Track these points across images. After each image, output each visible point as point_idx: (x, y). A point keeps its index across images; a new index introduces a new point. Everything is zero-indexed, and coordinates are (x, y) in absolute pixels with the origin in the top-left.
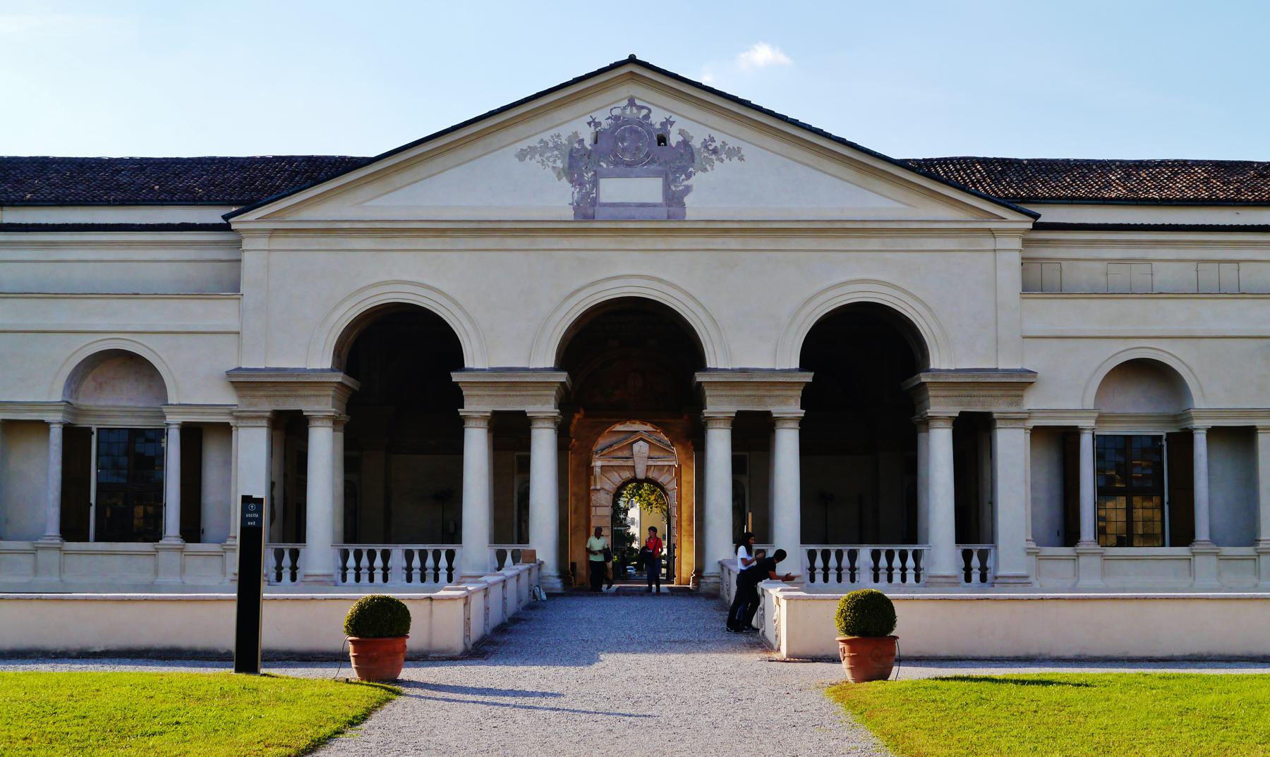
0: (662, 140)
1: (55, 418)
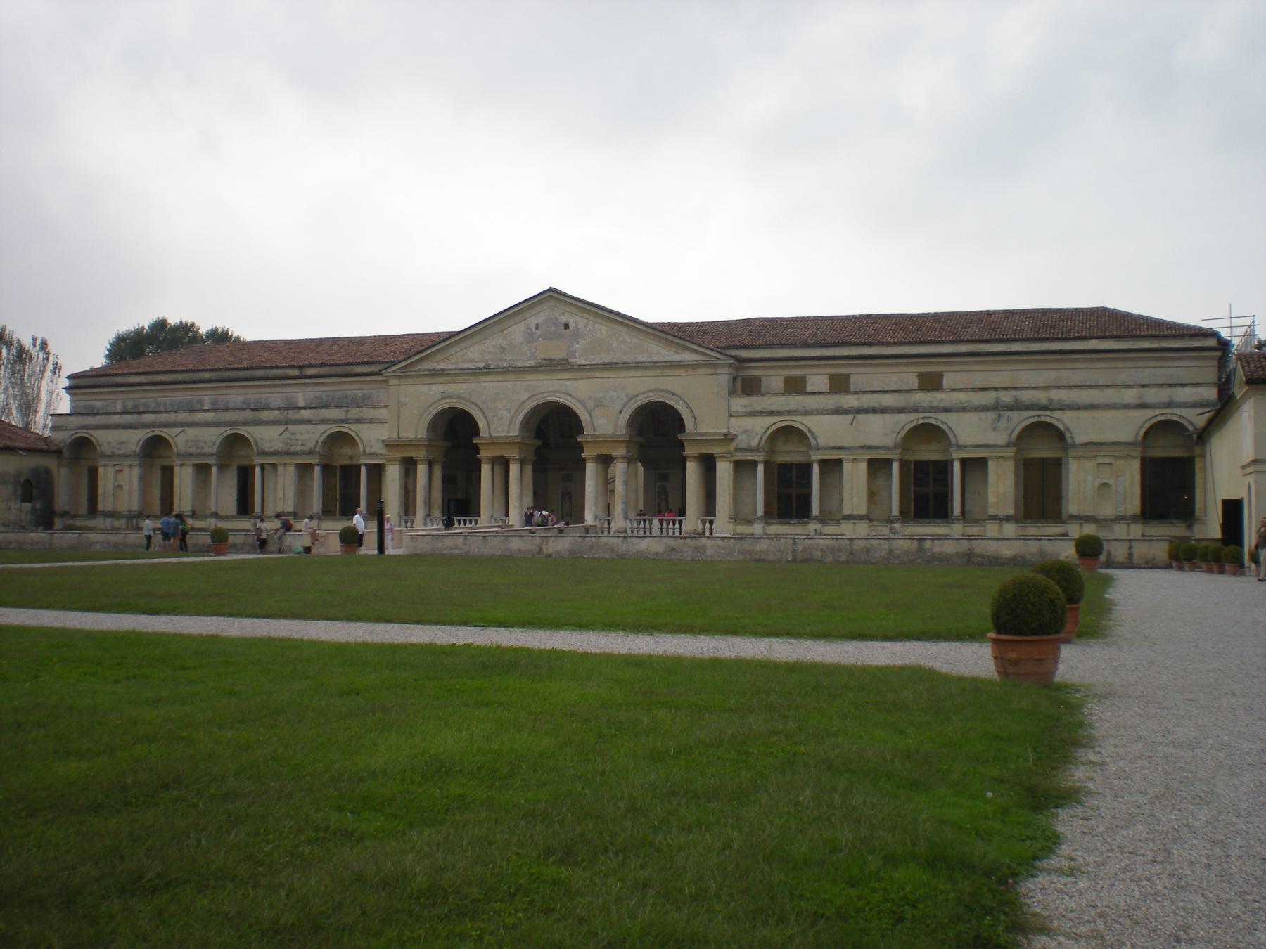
0: (567, 326)
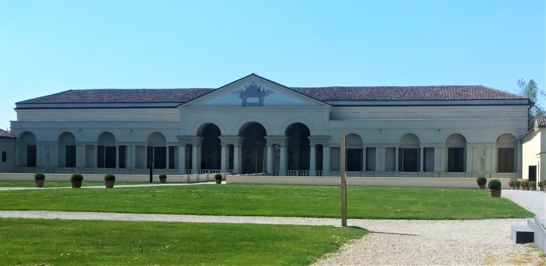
0: (259, 90)
1: (146, 145)
